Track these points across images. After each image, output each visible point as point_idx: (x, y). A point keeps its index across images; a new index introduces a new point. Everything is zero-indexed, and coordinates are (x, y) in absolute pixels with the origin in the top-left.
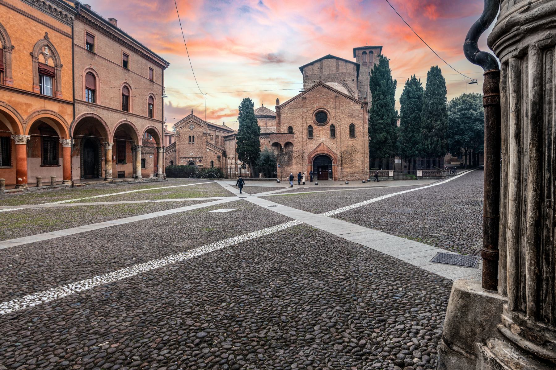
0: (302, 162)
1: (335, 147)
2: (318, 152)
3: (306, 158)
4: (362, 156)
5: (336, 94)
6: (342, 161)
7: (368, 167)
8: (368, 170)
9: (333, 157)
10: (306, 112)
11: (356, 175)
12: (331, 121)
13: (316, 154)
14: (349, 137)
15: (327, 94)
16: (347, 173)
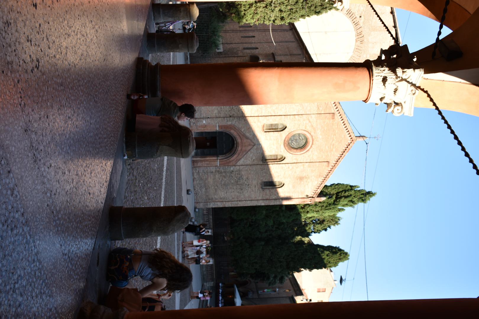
0: (222, 115)
1: (249, 162)
2: (239, 141)
3: (229, 123)
4: (233, 198)
5: (333, 162)
6: (225, 172)
7: (216, 206)
8: (212, 205)
9: (232, 159)
10: (309, 120)
11: (204, 190)
12: (290, 156)
13: (237, 137)
14: (264, 180)
15: (334, 150)
16: (207, 179)
